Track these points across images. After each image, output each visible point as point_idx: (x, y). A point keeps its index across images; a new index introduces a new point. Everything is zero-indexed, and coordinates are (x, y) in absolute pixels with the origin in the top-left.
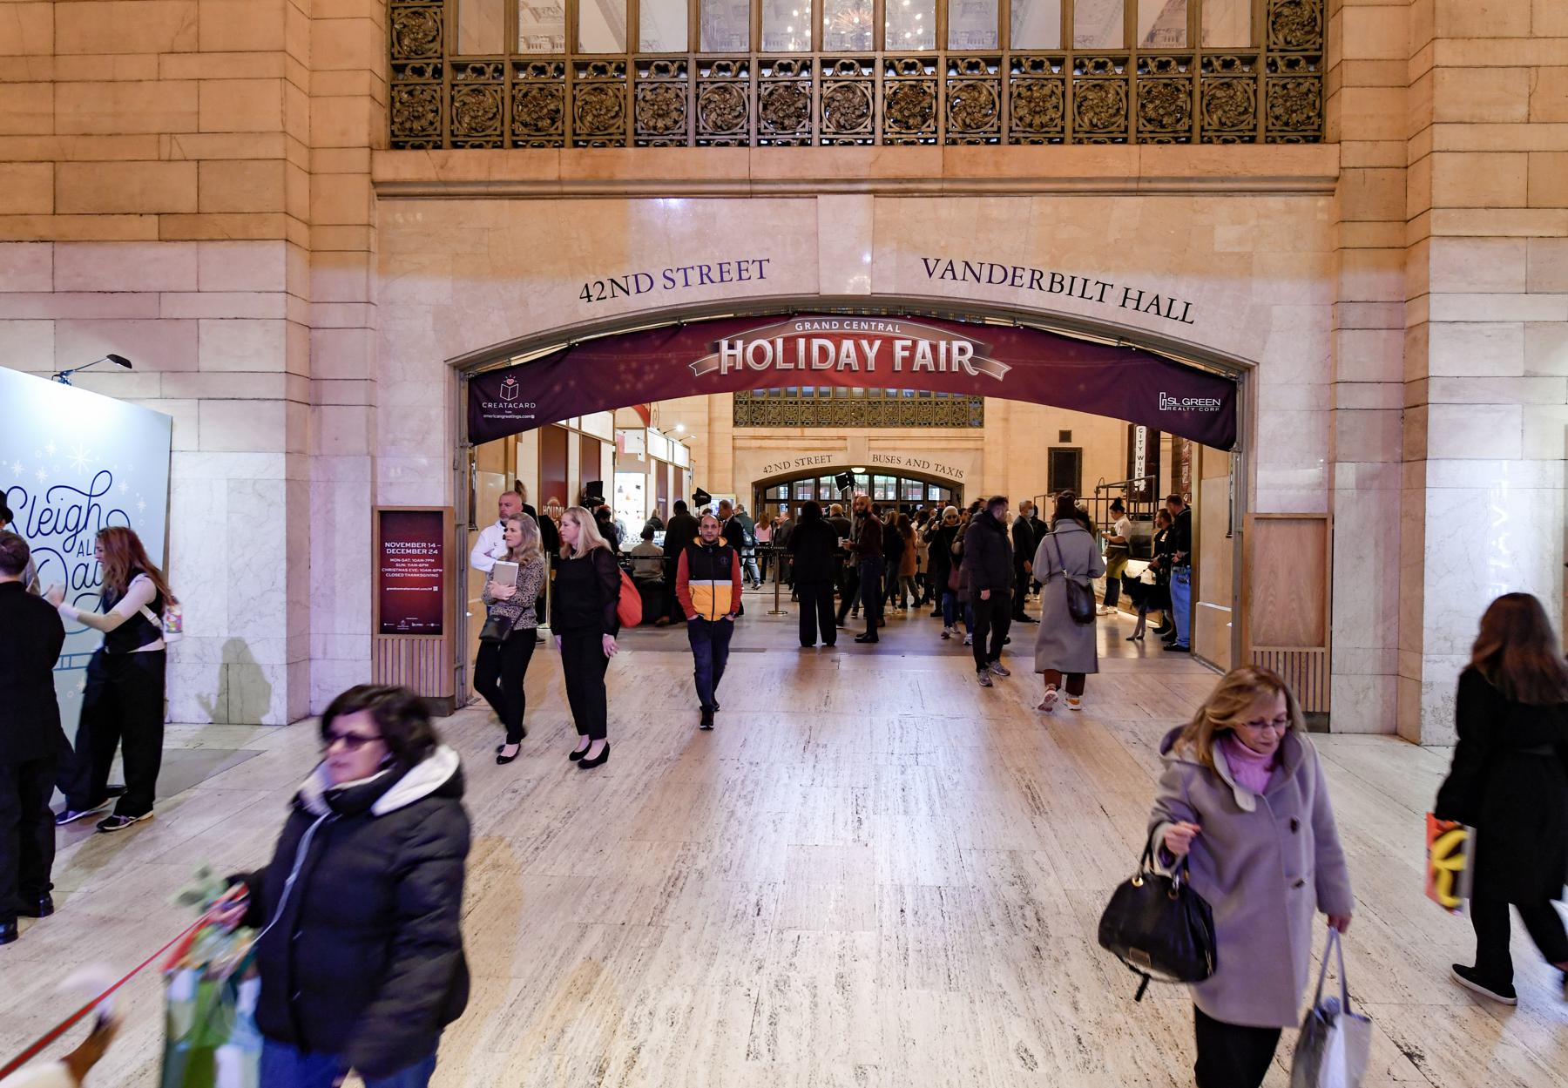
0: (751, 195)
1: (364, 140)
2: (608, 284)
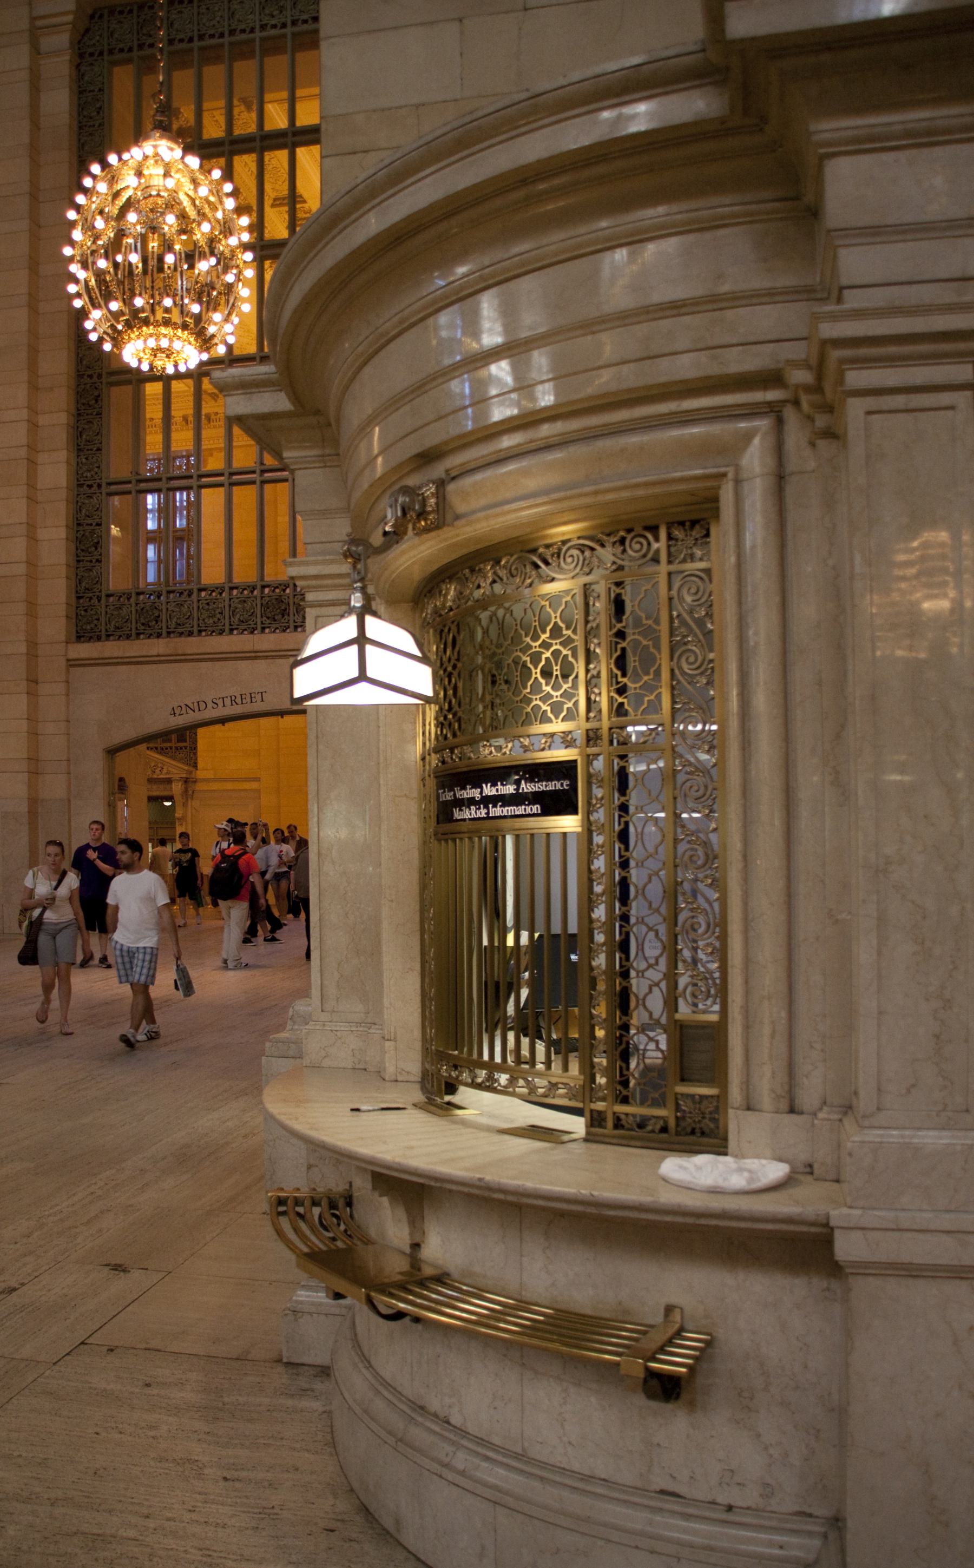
0: (256, 658)
1: (64, 638)
2: (184, 707)
